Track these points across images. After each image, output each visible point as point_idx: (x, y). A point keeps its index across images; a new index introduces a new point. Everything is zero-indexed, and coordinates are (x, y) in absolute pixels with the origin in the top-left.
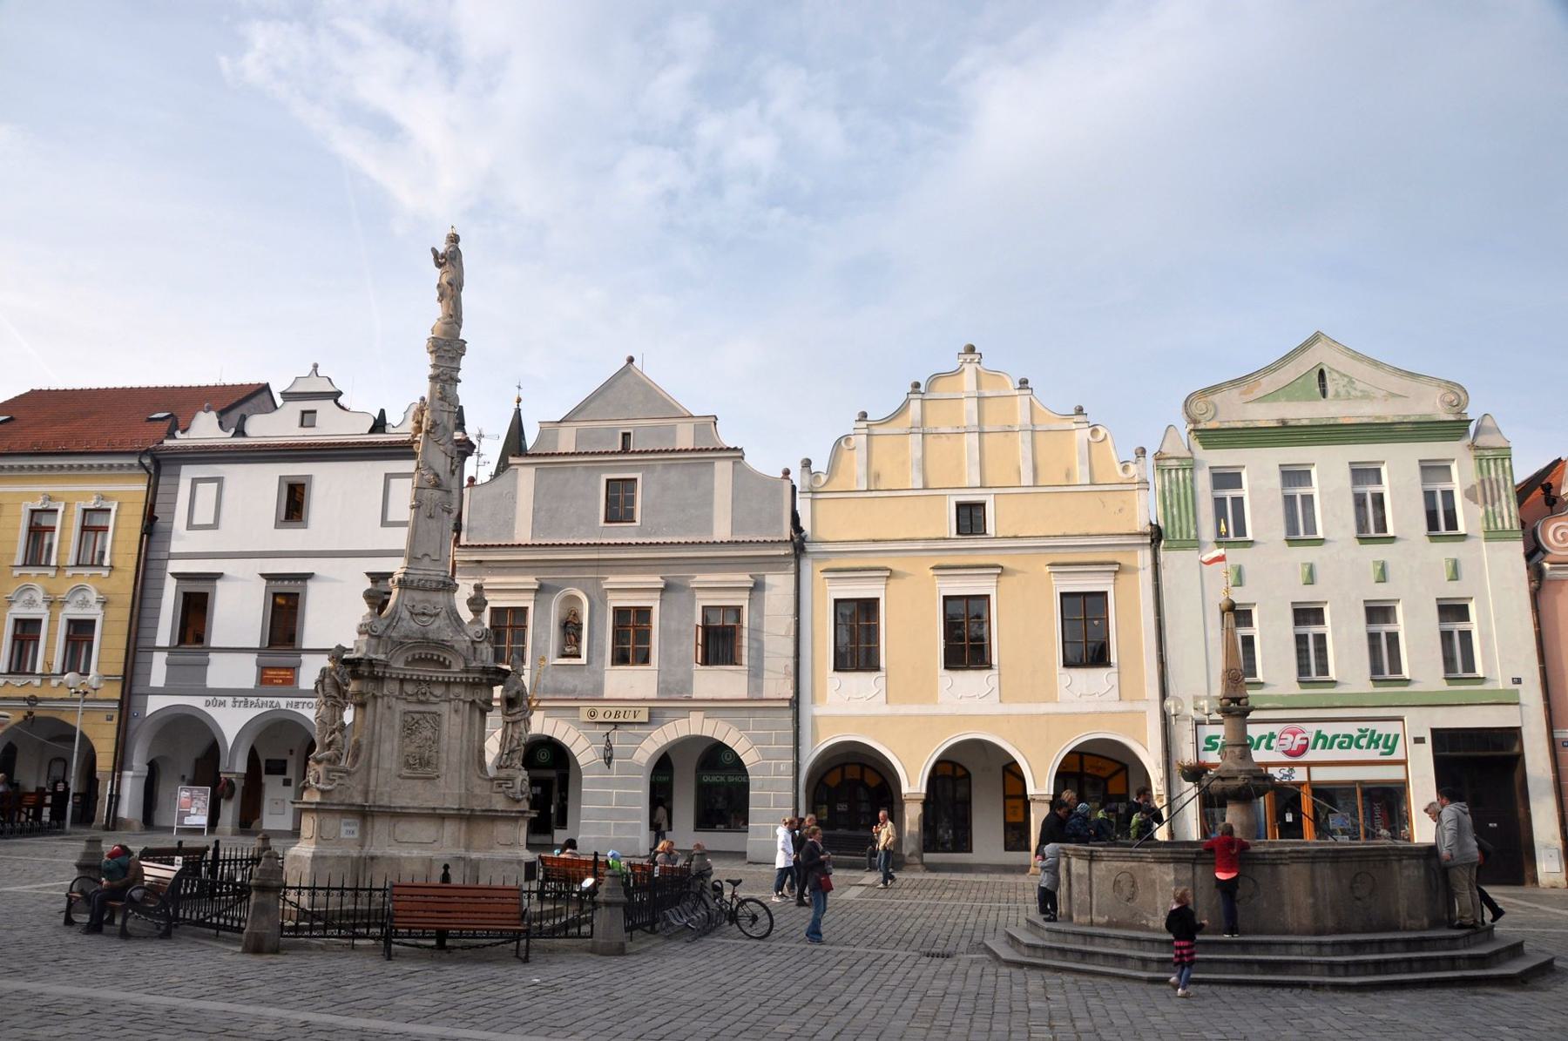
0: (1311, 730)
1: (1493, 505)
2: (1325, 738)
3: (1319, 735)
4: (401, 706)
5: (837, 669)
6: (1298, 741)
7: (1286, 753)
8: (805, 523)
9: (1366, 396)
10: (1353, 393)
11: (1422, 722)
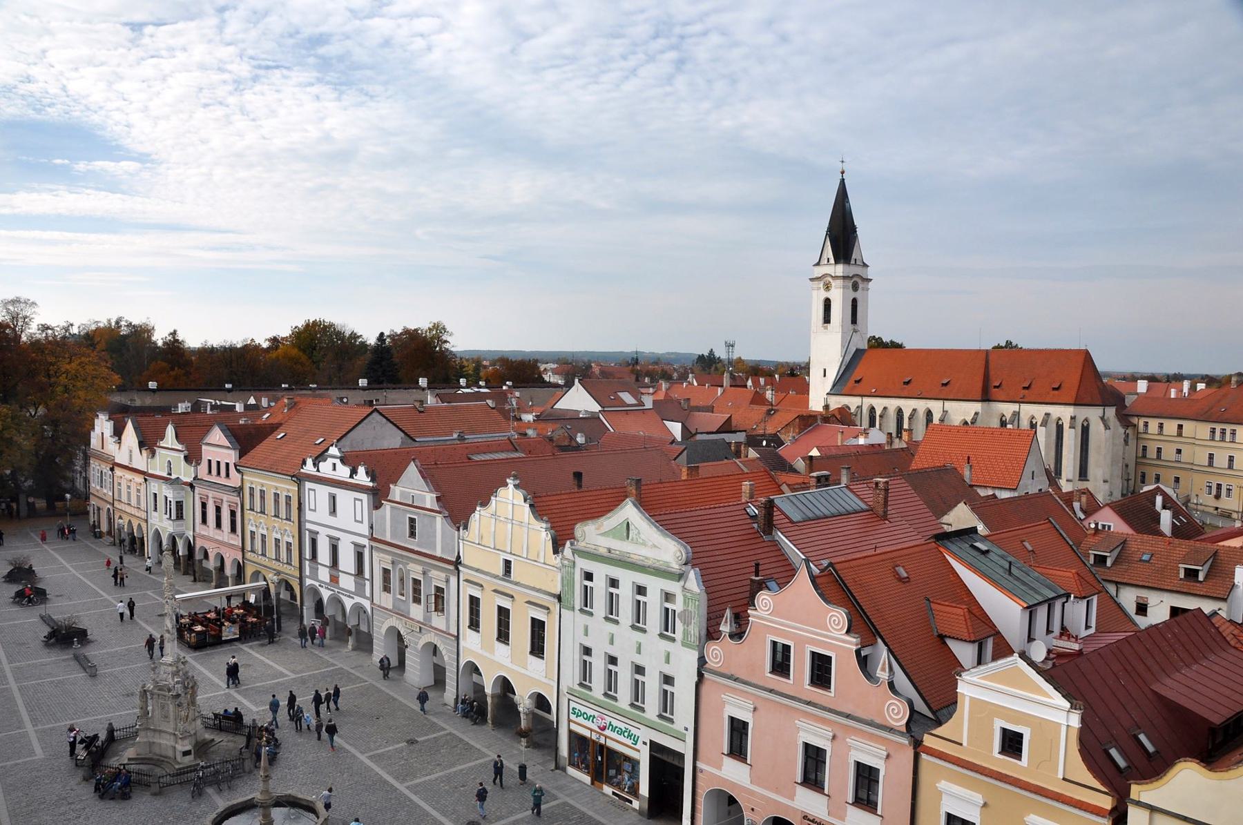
0: (608, 719)
1: (688, 626)
2: (612, 726)
3: (610, 724)
4: (160, 701)
5: (469, 627)
8: (461, 554)
9: (644, 544)
11: (646, 735)
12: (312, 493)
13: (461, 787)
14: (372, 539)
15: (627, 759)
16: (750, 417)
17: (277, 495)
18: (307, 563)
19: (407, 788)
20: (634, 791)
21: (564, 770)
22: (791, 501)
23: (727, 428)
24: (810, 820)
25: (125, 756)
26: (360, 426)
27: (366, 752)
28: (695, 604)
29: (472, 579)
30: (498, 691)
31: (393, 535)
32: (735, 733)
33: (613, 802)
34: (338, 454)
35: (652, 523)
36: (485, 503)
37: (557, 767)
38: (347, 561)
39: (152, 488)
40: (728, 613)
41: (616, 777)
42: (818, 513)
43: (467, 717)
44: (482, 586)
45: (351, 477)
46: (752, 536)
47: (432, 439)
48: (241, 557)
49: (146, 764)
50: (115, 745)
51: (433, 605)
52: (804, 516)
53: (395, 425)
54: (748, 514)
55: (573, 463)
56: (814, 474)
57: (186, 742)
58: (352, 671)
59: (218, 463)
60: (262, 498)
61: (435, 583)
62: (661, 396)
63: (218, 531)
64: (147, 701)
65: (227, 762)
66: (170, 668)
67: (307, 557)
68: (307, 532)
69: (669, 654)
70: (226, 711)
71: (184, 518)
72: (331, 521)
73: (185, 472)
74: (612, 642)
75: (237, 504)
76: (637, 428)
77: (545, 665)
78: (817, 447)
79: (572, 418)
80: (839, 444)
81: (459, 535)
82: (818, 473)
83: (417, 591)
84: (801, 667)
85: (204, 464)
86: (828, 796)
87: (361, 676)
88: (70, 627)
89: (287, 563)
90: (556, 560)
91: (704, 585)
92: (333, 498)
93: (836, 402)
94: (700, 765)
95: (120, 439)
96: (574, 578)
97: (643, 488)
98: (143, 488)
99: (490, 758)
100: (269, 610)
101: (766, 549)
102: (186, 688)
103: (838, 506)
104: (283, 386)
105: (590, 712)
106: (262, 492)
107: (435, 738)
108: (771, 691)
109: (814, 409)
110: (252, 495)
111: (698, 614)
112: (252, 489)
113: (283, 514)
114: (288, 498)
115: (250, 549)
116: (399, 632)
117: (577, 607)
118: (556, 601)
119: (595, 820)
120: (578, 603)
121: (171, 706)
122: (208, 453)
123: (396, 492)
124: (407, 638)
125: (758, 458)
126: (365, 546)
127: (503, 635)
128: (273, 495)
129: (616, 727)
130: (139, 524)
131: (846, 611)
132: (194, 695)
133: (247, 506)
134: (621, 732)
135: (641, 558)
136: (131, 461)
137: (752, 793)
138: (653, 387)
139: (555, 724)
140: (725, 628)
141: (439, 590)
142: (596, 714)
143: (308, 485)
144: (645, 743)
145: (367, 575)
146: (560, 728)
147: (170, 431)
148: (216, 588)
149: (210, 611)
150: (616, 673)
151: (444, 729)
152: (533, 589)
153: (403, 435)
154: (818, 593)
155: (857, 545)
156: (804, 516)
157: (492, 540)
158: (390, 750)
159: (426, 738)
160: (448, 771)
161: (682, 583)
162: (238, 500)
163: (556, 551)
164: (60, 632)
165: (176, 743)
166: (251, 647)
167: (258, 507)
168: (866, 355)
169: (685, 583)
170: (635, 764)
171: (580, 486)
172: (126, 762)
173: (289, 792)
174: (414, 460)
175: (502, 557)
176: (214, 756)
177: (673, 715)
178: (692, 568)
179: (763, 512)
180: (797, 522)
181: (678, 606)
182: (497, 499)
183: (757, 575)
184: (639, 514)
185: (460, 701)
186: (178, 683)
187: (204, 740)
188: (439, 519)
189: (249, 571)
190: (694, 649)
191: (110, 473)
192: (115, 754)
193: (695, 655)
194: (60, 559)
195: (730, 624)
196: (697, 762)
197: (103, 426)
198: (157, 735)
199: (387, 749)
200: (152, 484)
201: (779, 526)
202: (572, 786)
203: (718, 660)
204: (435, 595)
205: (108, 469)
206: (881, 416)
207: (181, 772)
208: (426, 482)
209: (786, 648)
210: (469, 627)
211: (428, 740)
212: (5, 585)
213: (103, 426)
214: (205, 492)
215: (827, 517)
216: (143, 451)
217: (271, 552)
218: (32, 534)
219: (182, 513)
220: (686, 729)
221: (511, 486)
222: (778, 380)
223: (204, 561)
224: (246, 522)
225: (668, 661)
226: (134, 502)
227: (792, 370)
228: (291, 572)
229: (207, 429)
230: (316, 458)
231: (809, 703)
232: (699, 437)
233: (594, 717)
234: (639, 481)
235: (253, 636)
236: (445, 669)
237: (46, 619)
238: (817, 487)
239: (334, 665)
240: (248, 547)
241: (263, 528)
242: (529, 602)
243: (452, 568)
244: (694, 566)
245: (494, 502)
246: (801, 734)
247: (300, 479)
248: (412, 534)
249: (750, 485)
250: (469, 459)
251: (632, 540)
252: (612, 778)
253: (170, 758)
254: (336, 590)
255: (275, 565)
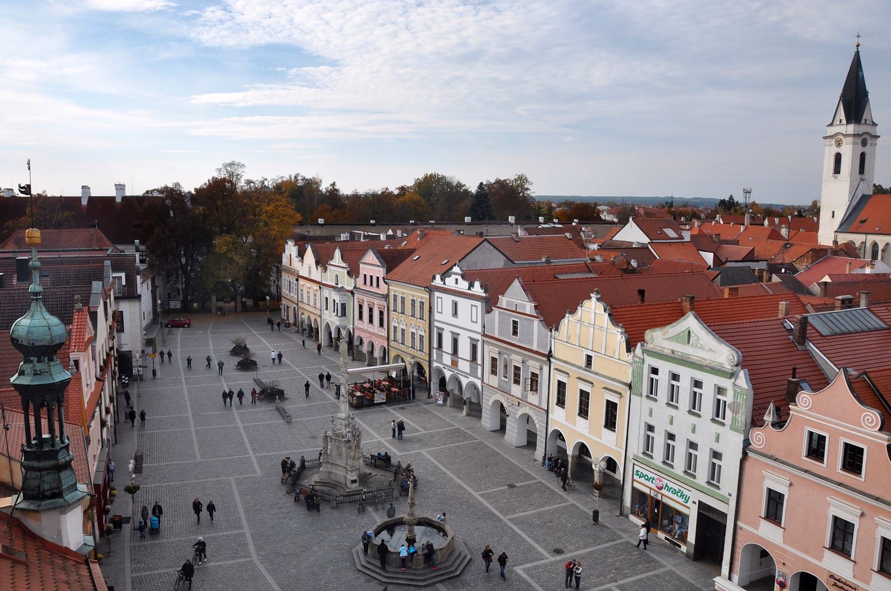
0: (665, 482)
1: (736, 415)
5: (557, 404)
6: (660, 485)
7: (657, 487)
8: (553, 349)
9: (702, 348)
10: (698, 345)
11: (696, 496)
12: (439, 300)
13: (549, 522)
14: (484, 335)
15: (679, 513)
16: (769, 249)
17: (413, 301)
18: (435, 350)
19: (509, 519)
20: (683, 538)
21: (627, 517)
22: (821, 319)
23: (750, 257)
24: (836, 580)
25: (312, 480)
26: (475, 251)
27: (478, 491)
28: (743, 397)
29: (559, 368)
30: (577, 453)
31: (500, 333)
32: (771, 501)
33: (665, 546)
34: (460, 272)
35: (709, 332)
36: (573, 311)
37: (621, 514)
38: (464, 350)
39: (325, 293)
40: (771, 406)
41: (668, 526)
42: (844, 329)
43: (552, 471)
44: (568, 374)
45: (469, 289)
46: (789, 346)
47: (526, 262)
48: (387, 344)
49: (326, 486)
50: (306, 472)
51: (529, 386)
52: (832, 332)
53: (499, 251)
54: (785, 327)
55: (636, 283)
56: (840, 297)
57: (354, 473)
58: (467, 431)
59: (371, 277)
60: (403, 302)
61: (531, 370)
62: (696, 232)
63: (370, 325)
64: (327, 443)
65: (381, 490)
66: (344, 422)
67: (435, 346)
68: (435, 328)
69: (718, 435)
70: (379, 454)
71: (347, 315)
72: (453, 321)
73: (347, 283)
74: (671, 423)
75: (384, 306)
76: (676, 256)
77: (615, 437)
78: (829, 275)
79: (627, 248)
80: (847, 273)
81: (551, 335)
82: (843, 296)
83: (517, 376)
84: (834, 455)
85: (361, 277)
86: (854, 562)
87: (474, 435)
88: (274, 388)
89: (420, 350)
90: (629, 357)
91: (751, 382)
92: (455, 305)
93: (843, 238)
94: (739, 524)
95: (302, 259)
96: (642, 372)
97: (695, 303)
98: (318, 294)
99: (569, 503)
100: (407, 383)
101: (802, 357)
102: (354, 436)
103: (861, 324)
104: (411, 222)
105: (650, 475)
106: (403, 299)
107: (528, 485)
108: (806, 471)
109: (822, 244)
110: (395, 300)
111: (745, 406)
112: (395, 296)
113: (418, 315)
114: (422, 303)
115: (393, 339)
116: (502, 405)
117: (645, 393)
118: (627, 388)
119: (651, 557)
120: (645, 390)
121: (344, 449)
122: (364, 269)
123: (503, 301)
124: (508, 410)
125: (780, 282)
126: (478, 340)
127: (584, 412)
128: (410, 301)
129: (671, 488)
130: (315, 319)
131: (880, 412)
132: (359, 442)
133: (392, 308)
134: (675, 492)
135: (699, 359)
136: (310, 274)
137: (784, 551)
138: (688, 224)
139: (622, 482)
140: (769, 418)
141: (534, 375)
142: (656, 477)
143: (437, 294)
144: (694, 503)
145: (479, 361)
146: (625, 485)
147: (337, 253)
148: (368, 366)
149: (365, 382)
150: (674, 447)
151: (535, 479)
152: (609, 378)
153: (505, 258)
154: (853, 395)
155: (879, 357)
156: (831, 330)
157: (578, 340)
158: (496, 491)
159: (522, 484)
160: (539, 510)
161: (733, 380)
162: (385, 304)
163: (629, 350)
164: (267, 390)
165: (347, 473)
166: (394, 409)
167: (399, 309)
168: (871, 200)
169: (735, 380)
170: (685, 518)
171: (643, 301)
172: (313, 484)
173: (425, 516)
174: (517, 277)
175: (585, 353)
176: (372, 485)
177: (719, 483)
178: (742, 369)
179: (799, 326)
180: (826, 336)
181: (729, 398)
182: (583, 308)
183: (794, 377)
184: (700, 325)
185: (547, 458)
186: (349, 432)
187: (365, 473)
188: (536, 322)
189: (393, 354)
190: (741, 433)
191: (296, 282)
192: (307, 478)
193: (741, 438)
194: (264, 341)
195: (773, 415)
196: (738, 521)
197: (291, 249)
198: (334, 466)
199: (494, 490)
200: (325, 291)
201: (811, 339)
202: (634, 529)
203: (760, 443)
204: (531, 378)
205: (295, 279)
206: (883, 251)
207: (350, 495)
208: (527, 294)
209: (822, 439)
210: (557, 404)
211: (524, 486)
212: (231, 357)
213: (291, 249)
214: (361, 297)
215: (851, 333)
216: (319, 268)
217: (408, 342)
218: (246, 324)
219: (345, 312)
220: (730, 495)
221: (594, 299)
222: (790, 220)
223: (360, 346)
224: (391, 319)
225: (717, 440)
226: (312, 303)
227: (800, 212)
228: (423, 357)
229: (363, 253)
230: (443, 274)
231: (840, 484)
232: (729, 265)
233: (653, 479)
234: (692, 298)
235: (395, 401)
236: (536, 434)
237: (257, 382)
238: (842, 308)
239: (454, 426)
240: (392, 338)
241: (403, 324)
242: (605, 388)
243: (545, 359)
244: (743, 367)
245: (580, 311)
246: (831, 508)
247: (431, 290)
248: (515, 333)
249: (786, 304)
250: (556, 278)
251: (692, 344)
252: (665, 526)
253: (342, 484)
254: (456, 371)
255: (411, 351)
